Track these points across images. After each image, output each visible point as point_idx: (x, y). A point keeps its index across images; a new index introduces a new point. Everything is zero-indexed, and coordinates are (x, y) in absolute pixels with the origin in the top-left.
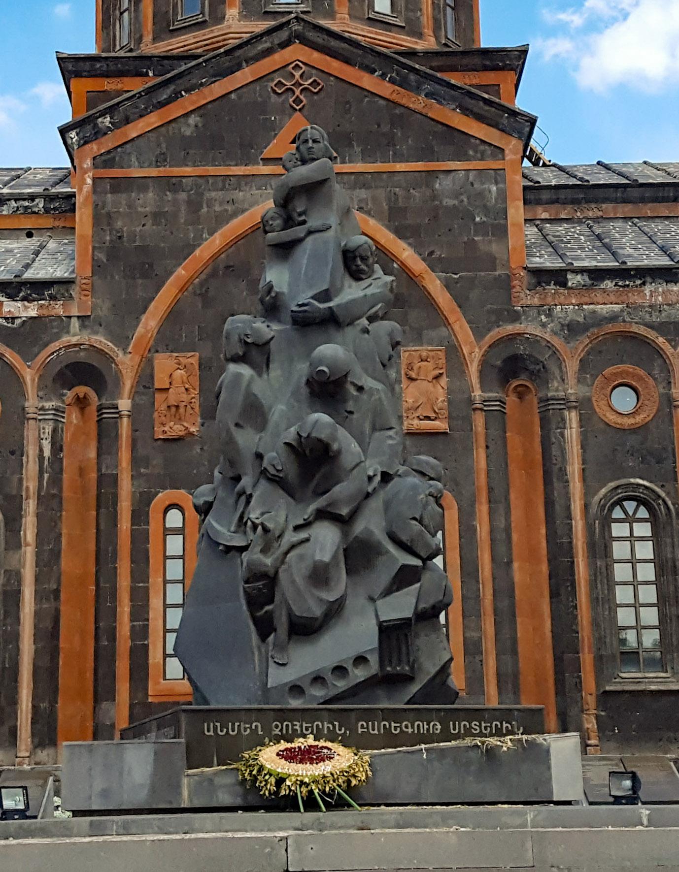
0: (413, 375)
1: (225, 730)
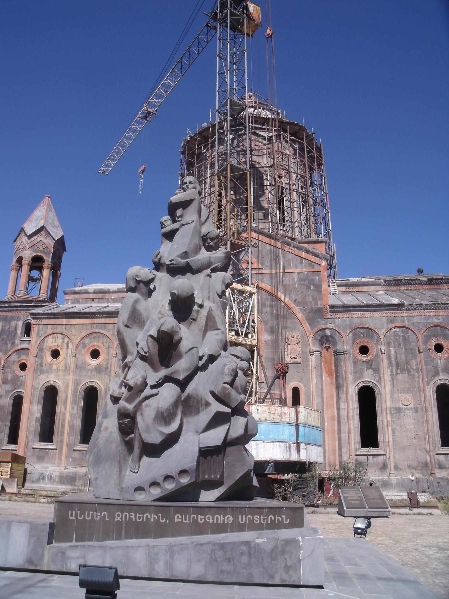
1: (83, 516)
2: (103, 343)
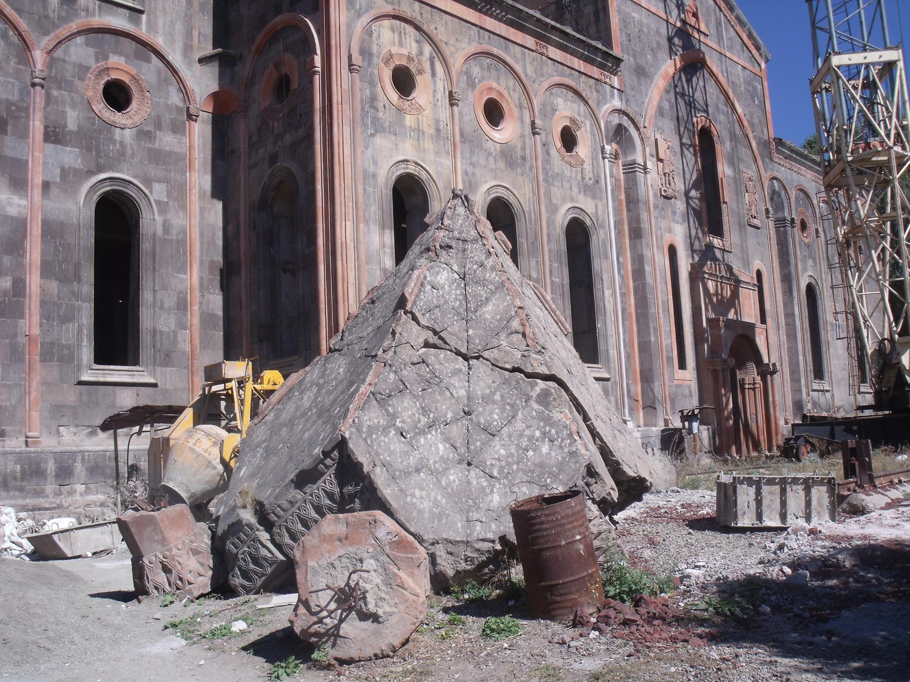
2: (507, 88)
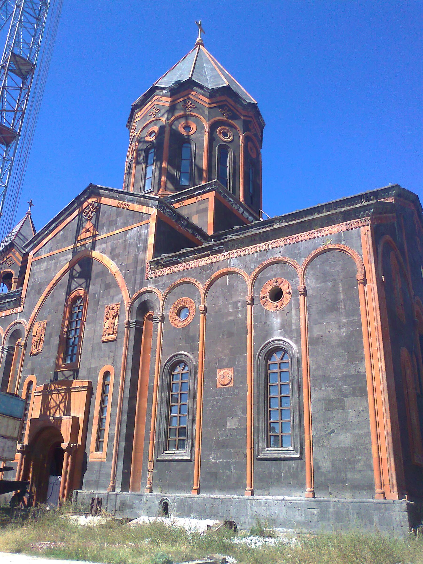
0: (108, 316)
